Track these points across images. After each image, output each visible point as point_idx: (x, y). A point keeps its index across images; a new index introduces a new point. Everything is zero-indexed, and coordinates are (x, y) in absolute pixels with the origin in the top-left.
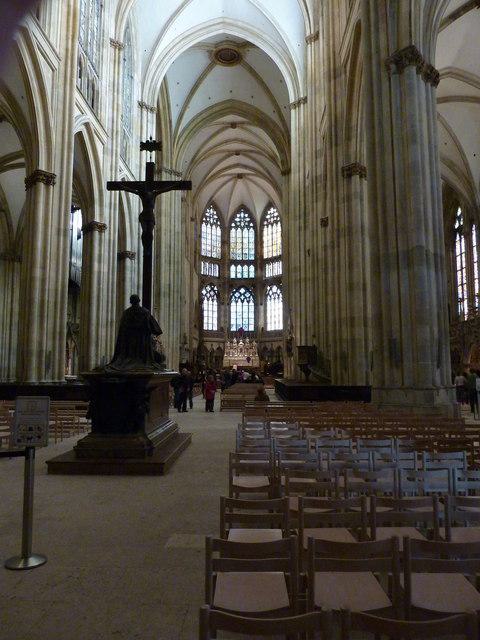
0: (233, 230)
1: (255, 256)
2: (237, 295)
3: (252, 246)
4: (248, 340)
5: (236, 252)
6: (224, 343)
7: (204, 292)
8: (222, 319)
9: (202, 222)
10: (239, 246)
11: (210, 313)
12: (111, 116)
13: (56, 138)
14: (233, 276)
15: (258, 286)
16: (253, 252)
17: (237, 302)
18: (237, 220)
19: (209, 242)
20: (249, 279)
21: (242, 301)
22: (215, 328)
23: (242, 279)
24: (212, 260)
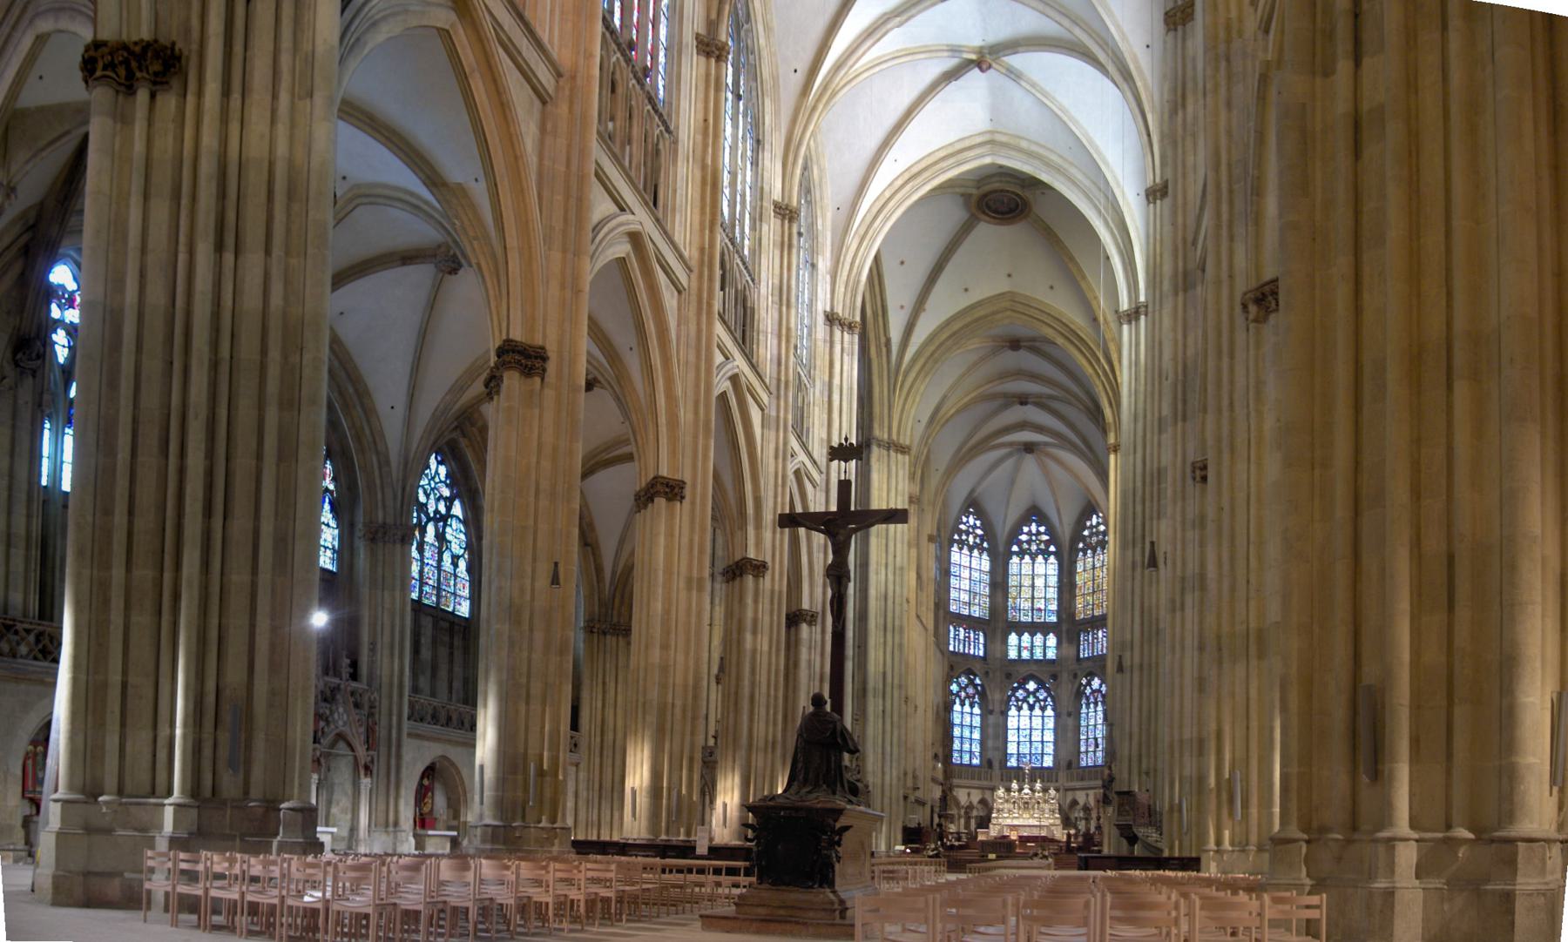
0: (1015, 559)
1: (1059, 613)
2: (1020, 694)
3: (1052, 593)
4: (1038, 786)
5: (1021, 606)
6: (993, 789)
8: (990, 743)
9: (951, 542)
10: (1026, 593)
11: (967, 733)
12: (775, 352)
13: (685, 415)
14: (1013, 654)
15: (1065, 677)
16: (1054, 607)
17: (1019, 709)
18: (1024, 538)
19: (965, 585)
20: (1045, 662)
21: (1031, 708)
22: (976, 761)
24: (971, 623)
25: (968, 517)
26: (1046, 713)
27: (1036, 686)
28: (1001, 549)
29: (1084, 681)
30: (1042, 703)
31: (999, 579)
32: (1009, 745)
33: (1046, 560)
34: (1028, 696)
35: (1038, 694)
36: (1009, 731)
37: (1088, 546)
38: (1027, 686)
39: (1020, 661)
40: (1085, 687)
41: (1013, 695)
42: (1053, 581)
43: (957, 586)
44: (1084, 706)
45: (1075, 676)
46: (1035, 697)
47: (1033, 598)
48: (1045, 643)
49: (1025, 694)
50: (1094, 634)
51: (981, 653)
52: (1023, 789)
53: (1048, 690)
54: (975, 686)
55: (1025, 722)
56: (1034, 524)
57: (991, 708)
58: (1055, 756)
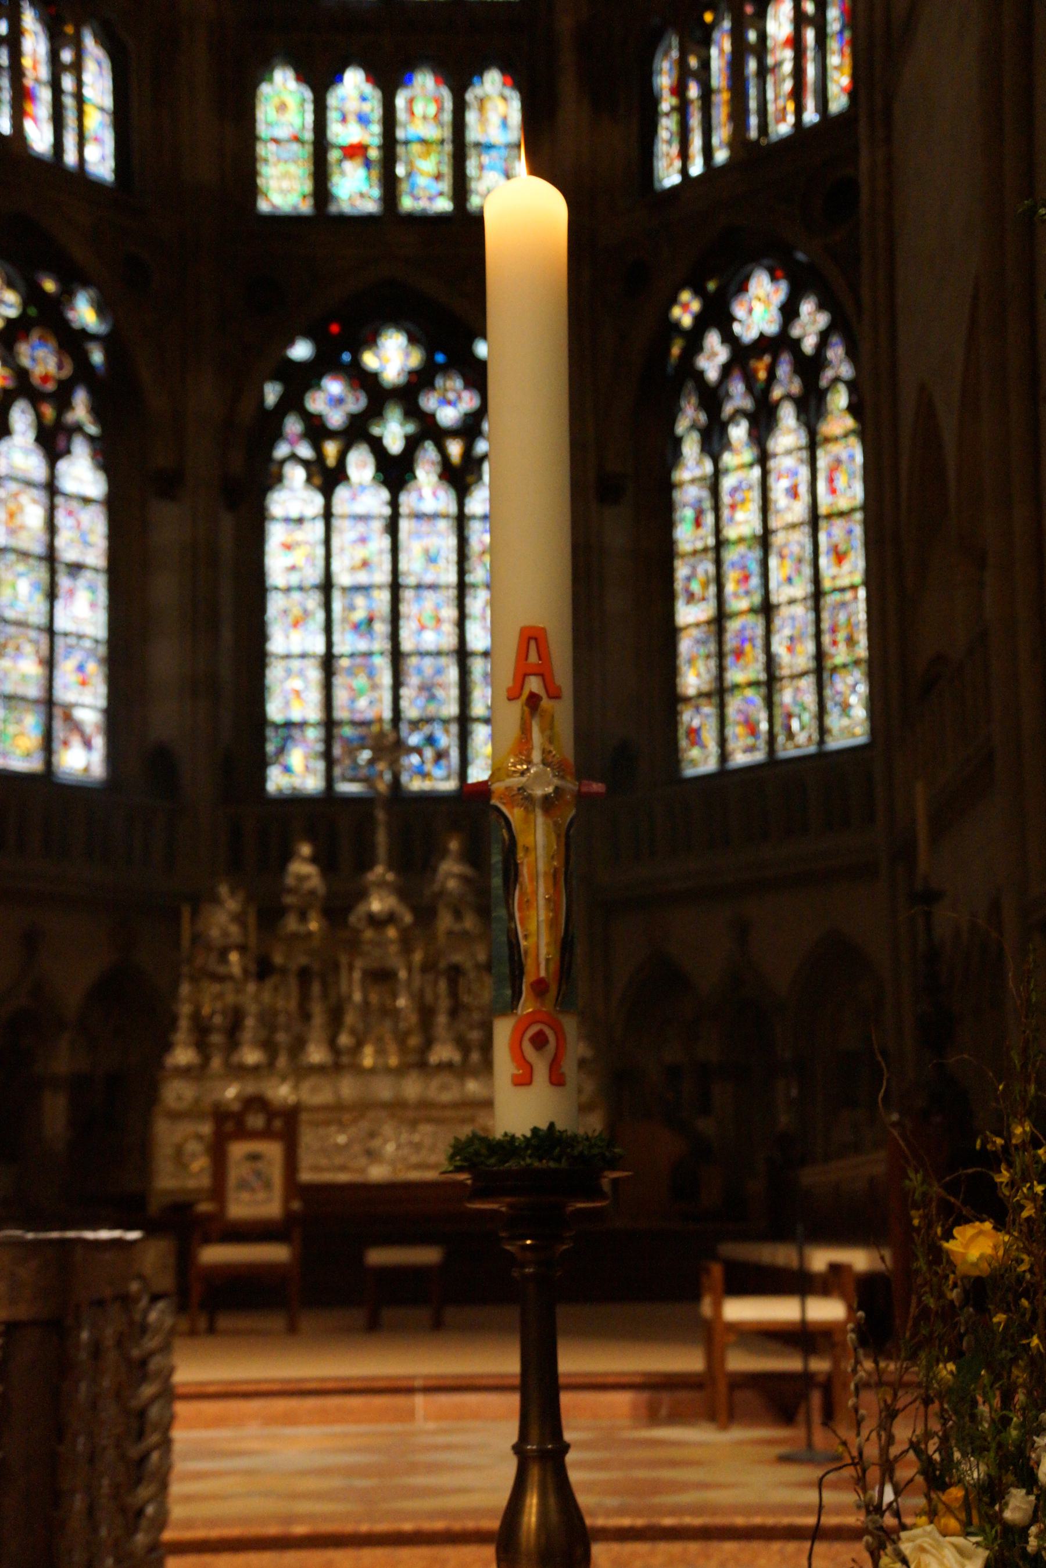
27: (415, 359)
30: (455, 449)
32: (274, 673)
34: (374, 411)
35: (429, 402)
36: (275, 604)
38: (370, 360)
41: (292, 402)
44: (691, 448)
46: (413, 412)
48: (459, 126)
49: (357, 403)
50: (737, 36)
52: (362, 895)
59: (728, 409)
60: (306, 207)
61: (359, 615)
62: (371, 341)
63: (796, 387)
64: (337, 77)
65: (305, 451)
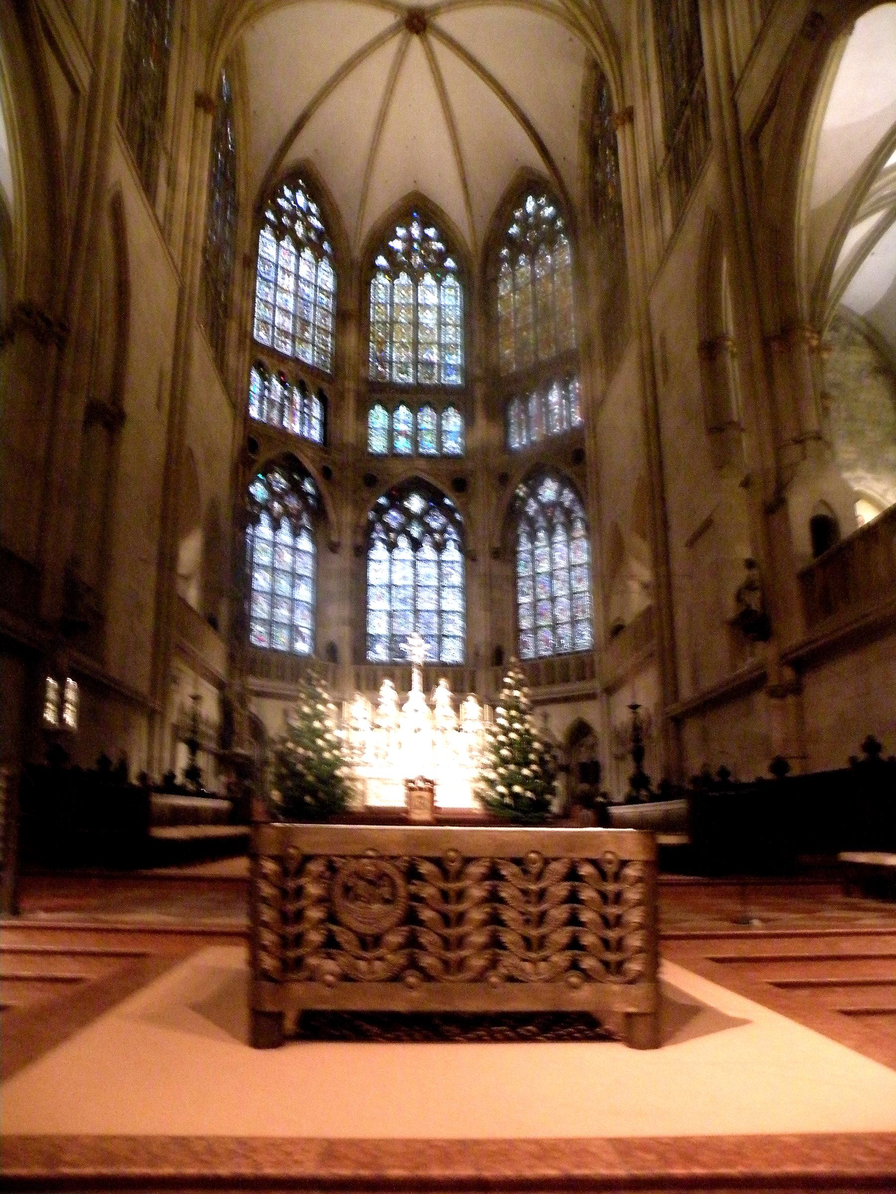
0: (382, 280)
1: (465, 371)
2: (393, 518)
3: (453, 335)
7: (258, 491)
9: (261, 222)
10: (403, 336)
11: (284, 586)
14: (378, 444)
16: (456, 359)
17: (392, 546)
18: (397, 245)
23: (417, 455)
25: (294, 193)
26: (446, 556)
28: (357, 253)
29: (521, 491)
31: (351, 305)
32: (371, 617)
33: (439, 281)
36: (372, 591)
37: (517, 246)
39: (393, 454)
40: (524, 501)
42: (454, 314)
43: (270, 300)
45: (504, 479)
47: (416, 343)
51: (316, 435)
53: (448, 512)
54: (303, 496)
55: (403, 574)
56: (415, 224)
57: (334, 538)
58: (467, 642)
59: (537, 525)
60: (385, 451)
61: (401, 596)
62: (407, 497)
63: (562, 519)
64: (396, 408)
65: (383, 536)
